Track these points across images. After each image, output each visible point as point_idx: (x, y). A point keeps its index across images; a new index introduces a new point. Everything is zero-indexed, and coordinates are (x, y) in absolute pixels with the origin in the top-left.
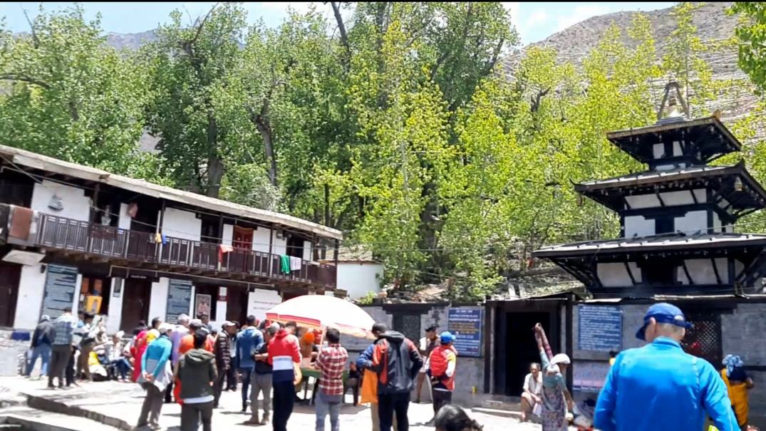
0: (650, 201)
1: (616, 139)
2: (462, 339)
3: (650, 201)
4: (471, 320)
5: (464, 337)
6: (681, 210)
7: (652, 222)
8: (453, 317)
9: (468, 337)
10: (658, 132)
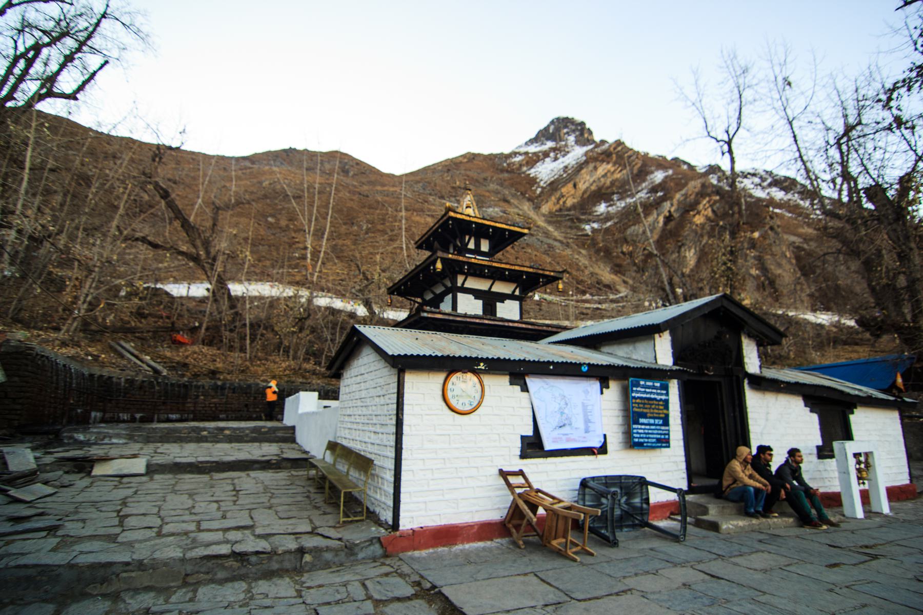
0: (482, 285)
3: (482, 285)
4: (659, 397)
5: (652, 421)
6: (503, 297)
7: (480, 302)
10: (490, 226)
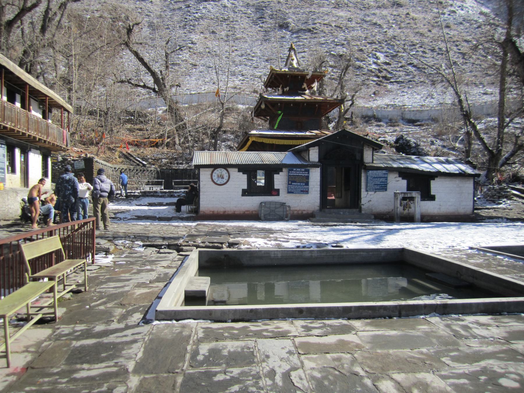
9: (302, 184)
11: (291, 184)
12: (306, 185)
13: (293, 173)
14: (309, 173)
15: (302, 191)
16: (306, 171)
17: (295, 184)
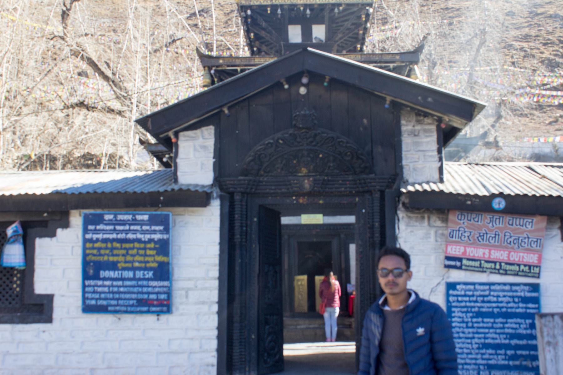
1: (250, 7)
2: (122, 279)
4: (148, 237)
5: (130, 274)
8: (96, 231)
9: (139, 274)
11: (96, 277)
12: (155, 278)
13: (105, 231)
14: (167, 230)
15: (141, 302)
16: (153, 221)
17: (111, 274)
